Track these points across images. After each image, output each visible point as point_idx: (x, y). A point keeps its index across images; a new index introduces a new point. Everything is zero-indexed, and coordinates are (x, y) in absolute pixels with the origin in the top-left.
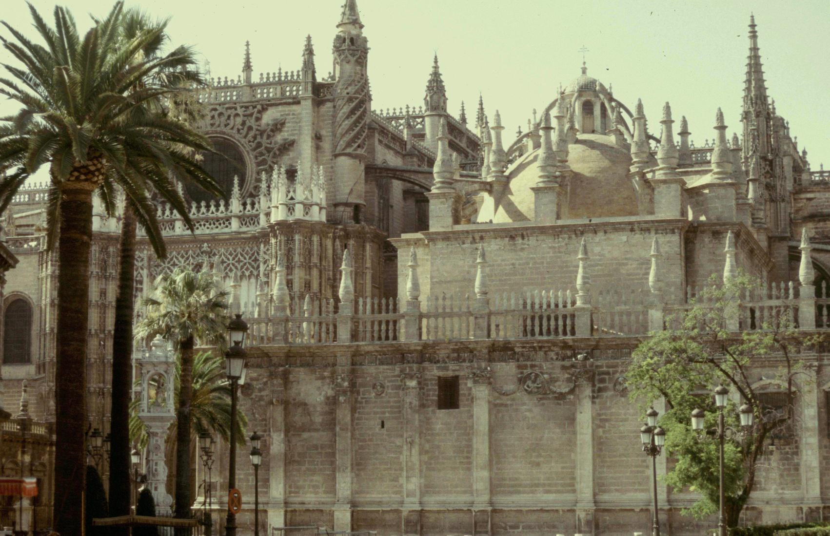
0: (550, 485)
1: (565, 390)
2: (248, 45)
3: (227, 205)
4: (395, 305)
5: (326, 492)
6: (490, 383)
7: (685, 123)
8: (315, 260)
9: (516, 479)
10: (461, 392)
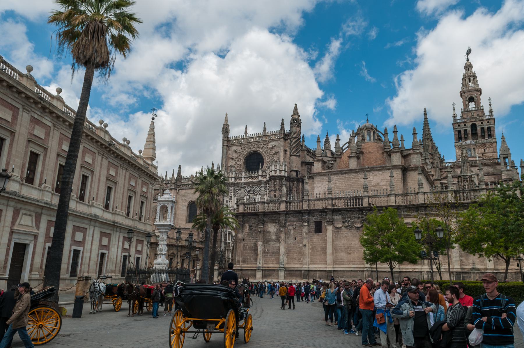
0: (354, 261)
1: (359, 226)
2: (265, 123)
3: (258, 172)
5: (276, 263)
6: (333, 224)
7: (402, 137)
9: (342, 259)
10: (323, 227)
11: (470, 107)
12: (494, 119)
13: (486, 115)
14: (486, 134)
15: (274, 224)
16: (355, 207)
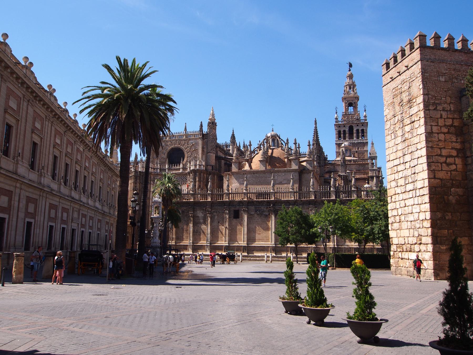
2: (186, 124)
3: (179, 165)
4: (223, 190)
8: (202, 179)
9: (254, 238)
11: (349, 111)
12: (367, 123)
13: (361, 119)
14: (360, 134)
15: (202, 211)
16: (264, 200)
